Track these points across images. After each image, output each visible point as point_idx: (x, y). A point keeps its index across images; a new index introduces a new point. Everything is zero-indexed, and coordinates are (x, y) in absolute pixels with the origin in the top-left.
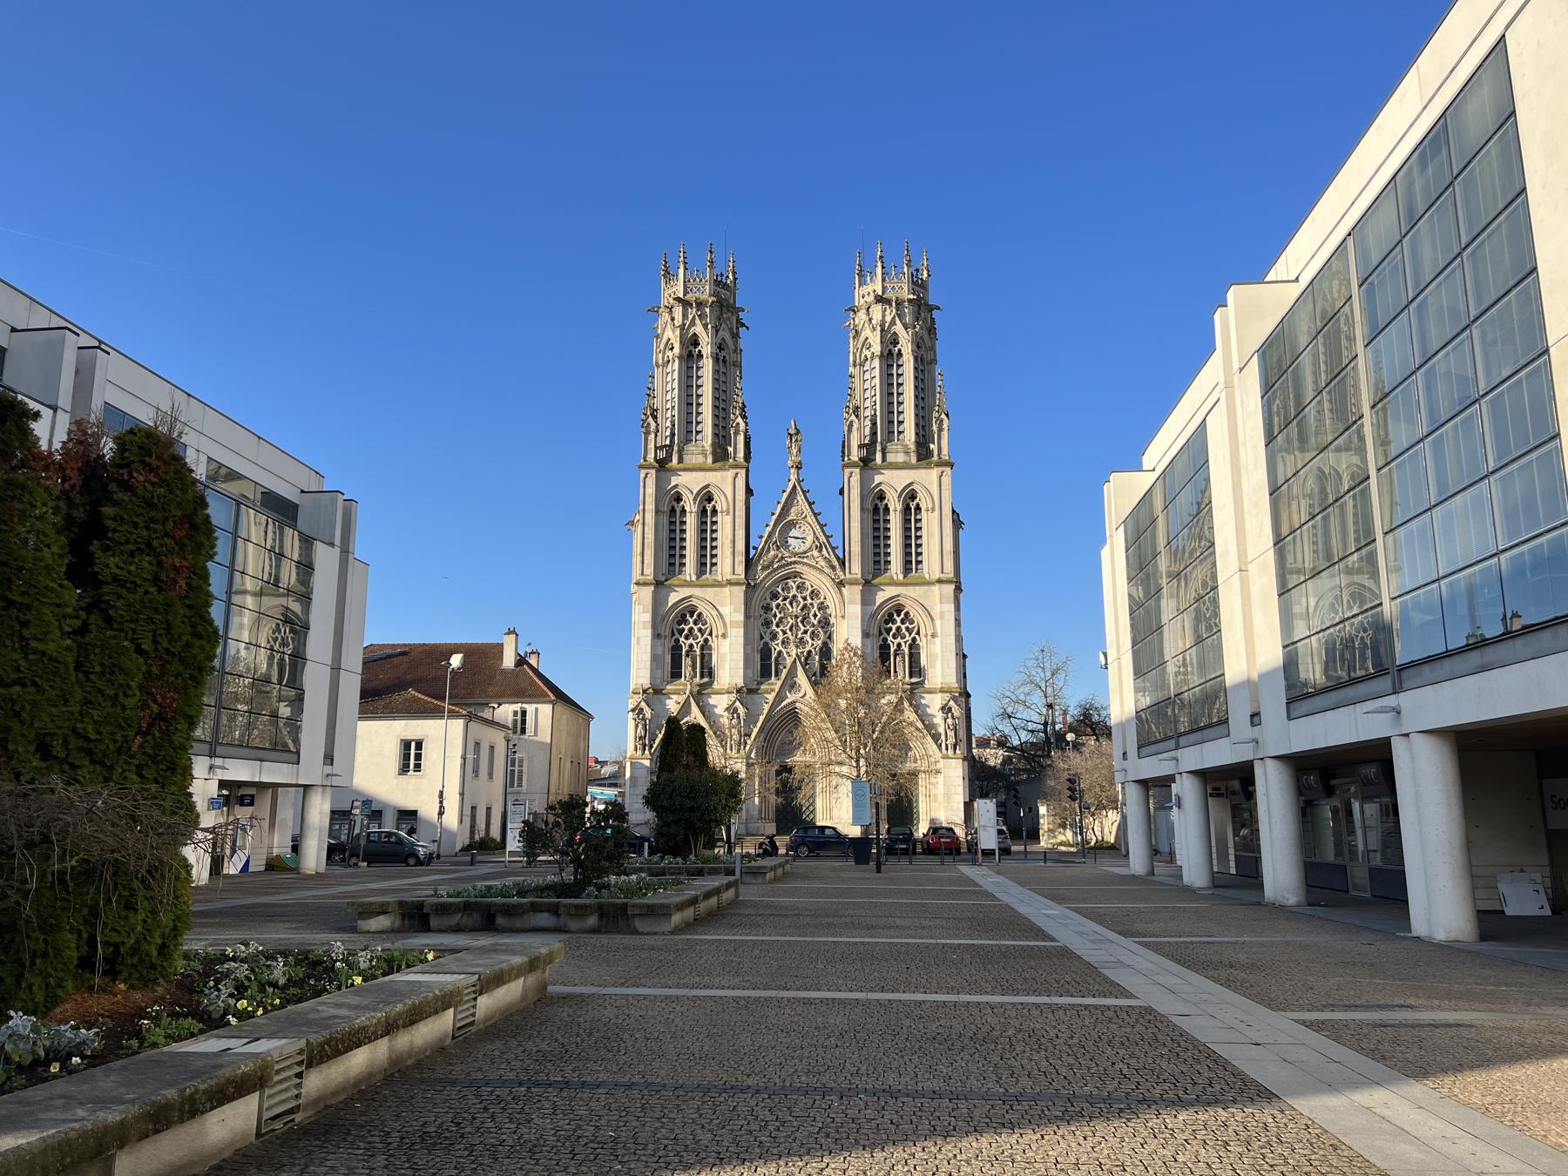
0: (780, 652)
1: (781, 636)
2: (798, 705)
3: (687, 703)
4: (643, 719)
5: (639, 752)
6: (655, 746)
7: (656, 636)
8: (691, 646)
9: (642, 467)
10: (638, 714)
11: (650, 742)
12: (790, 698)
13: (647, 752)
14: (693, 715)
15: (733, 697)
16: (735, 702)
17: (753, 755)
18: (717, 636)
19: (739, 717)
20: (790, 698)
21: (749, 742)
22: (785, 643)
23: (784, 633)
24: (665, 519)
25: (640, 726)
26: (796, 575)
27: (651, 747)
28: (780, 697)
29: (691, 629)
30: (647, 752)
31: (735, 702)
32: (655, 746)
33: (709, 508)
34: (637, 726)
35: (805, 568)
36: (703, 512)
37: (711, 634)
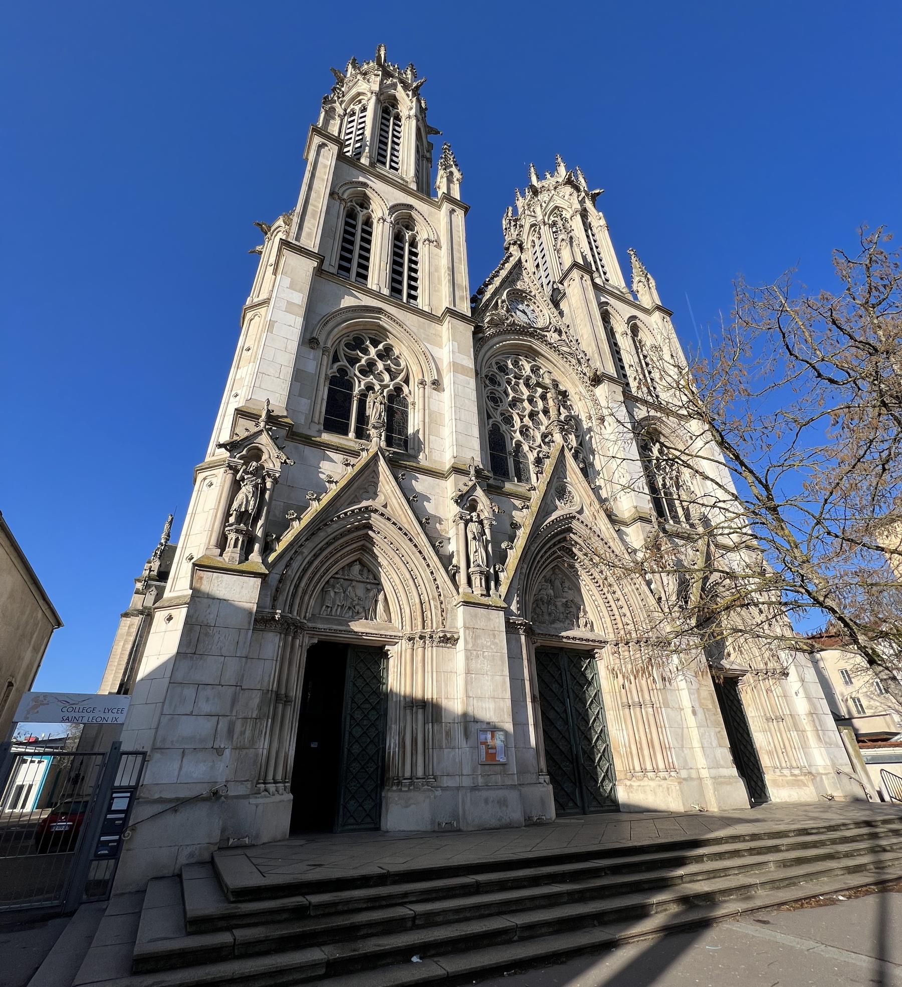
0: (519, 445)
1: (517, 424)
2: (575, 524)
3: (370, 467)
4: (259, 472)
5: (231, 555)
6: (280, 547)
7: (309, 341)
8: (370, 388)
9: (317, 131)
10: (247, 460)
11: (266, 534)
12: (562, 509)
13: (255, 556)
14: (381, 499)
15: (467, 482)
16: (473, 488)
17: (514, 607)
18: (422, 383)
19: (481, 522)
20: (562, 509)
21: (502, 576)
22: (524, 431)
23: (522, 420)
24: (341, 210)
25: (246, 490)
26: (532, 354)
27: (267, 549)
28: (545, 509)
29: (371, 364)
30: (255, 556)
31: (473, 488)
32: (280, 547)
33: (408, 235)
34: (236, 486)
35: (544, 347)
36: (398, 237)
37: (407, 381)
